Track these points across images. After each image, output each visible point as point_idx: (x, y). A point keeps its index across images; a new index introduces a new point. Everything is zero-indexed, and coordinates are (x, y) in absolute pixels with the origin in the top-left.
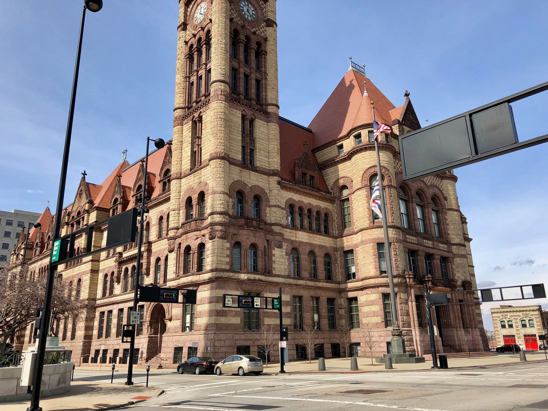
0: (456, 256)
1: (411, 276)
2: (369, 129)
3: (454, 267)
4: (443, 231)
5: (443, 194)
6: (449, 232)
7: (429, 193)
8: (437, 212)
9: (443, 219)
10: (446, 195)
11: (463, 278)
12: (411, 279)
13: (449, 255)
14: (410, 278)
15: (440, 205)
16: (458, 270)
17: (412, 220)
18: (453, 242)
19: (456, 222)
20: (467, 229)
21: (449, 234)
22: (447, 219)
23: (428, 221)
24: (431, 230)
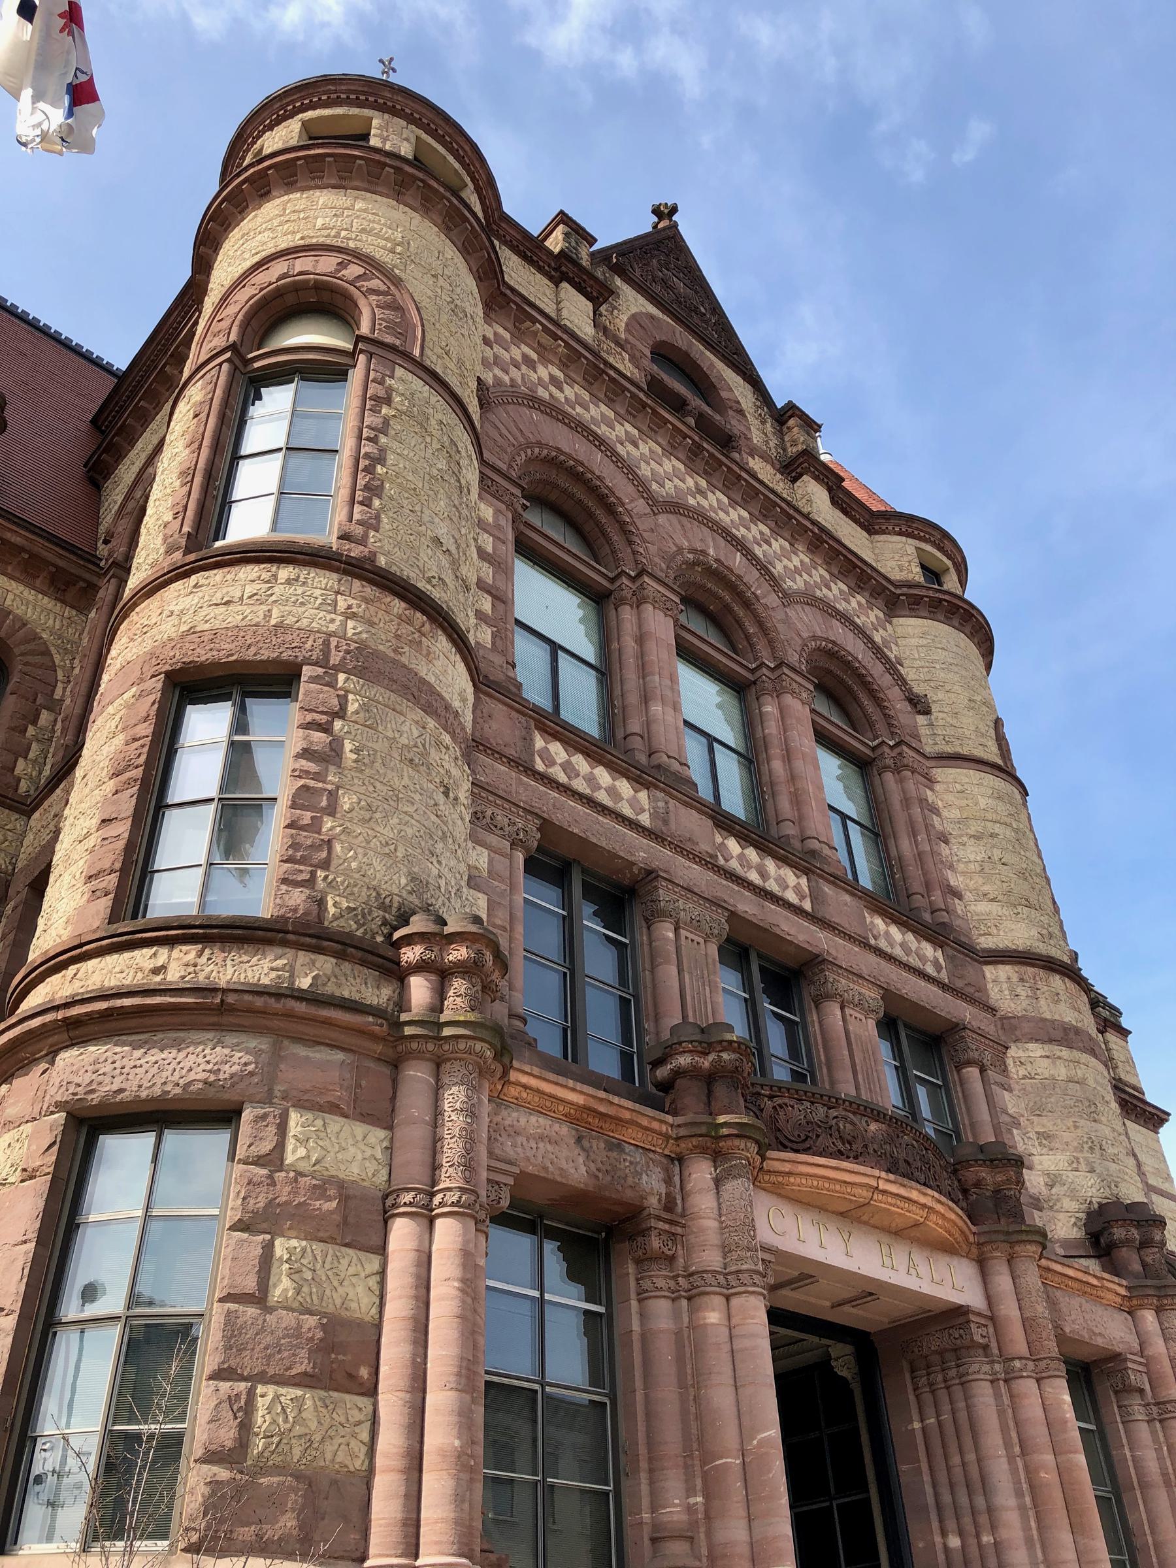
0: (1014, 1029)
1: (458, 953)
2: (310, 114)
3: (1011, 1103)
4: (913, 871)
5: (901, 681)
6: (955, 880)
7: (798, 628)
8: (862, 765)
9: (906, 802)
10: (918, 689)
11: (1091, 1189)
12: (458, 986)
13: (965, 1013)
14: (442, 974)
15: (881, 727)
16: (1046, 1124)
17: (633, 699)
18: (985, 943)
19: (997, 829)
20: (1130, 1061)
21: (958, 895)
22: (935, 811)
23: (777, 766)
24: (800, 821)
